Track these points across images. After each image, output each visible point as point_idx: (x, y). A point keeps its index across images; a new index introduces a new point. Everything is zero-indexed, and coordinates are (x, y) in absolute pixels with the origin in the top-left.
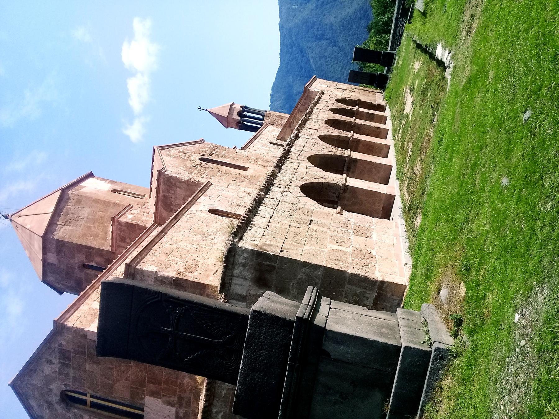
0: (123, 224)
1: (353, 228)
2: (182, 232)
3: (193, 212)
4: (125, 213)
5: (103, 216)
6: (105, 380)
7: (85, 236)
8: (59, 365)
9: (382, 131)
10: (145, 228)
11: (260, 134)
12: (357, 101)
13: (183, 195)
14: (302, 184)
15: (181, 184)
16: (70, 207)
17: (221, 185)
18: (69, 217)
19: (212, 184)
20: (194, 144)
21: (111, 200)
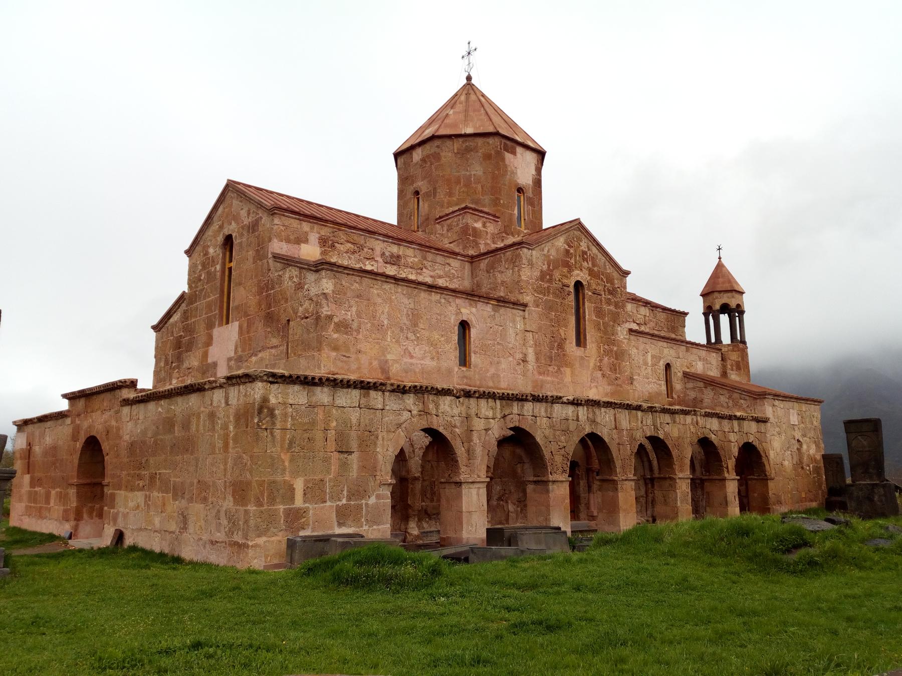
1: (352, 503)
2: (406, 301)
4: (483, 217)
5: (477, 192)
6: (244, 276)
8: (247, 223)
14: (441, 430)
19: (524, 311)
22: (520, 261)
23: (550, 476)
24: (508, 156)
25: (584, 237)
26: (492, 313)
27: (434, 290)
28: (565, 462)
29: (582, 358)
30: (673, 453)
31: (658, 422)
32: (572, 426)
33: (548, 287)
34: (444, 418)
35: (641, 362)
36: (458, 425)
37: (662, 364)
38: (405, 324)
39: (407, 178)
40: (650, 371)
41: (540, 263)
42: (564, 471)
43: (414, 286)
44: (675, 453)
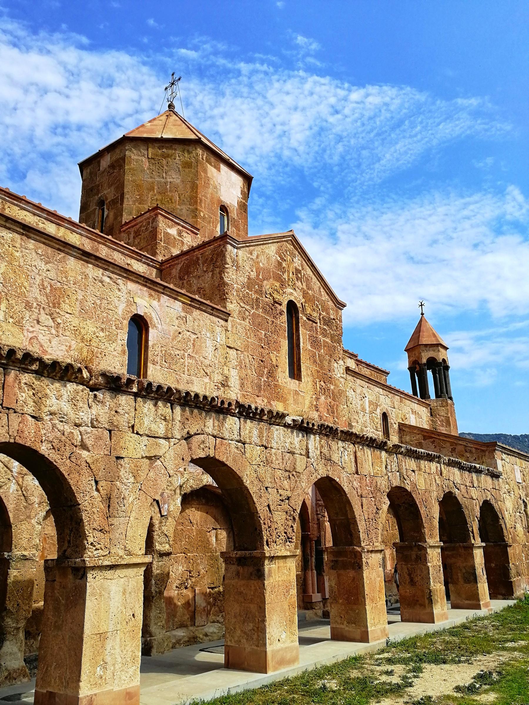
0: (154, 223)
2: (43, 266)
3: (122, 286)
4: (179, 224)
5: (173, 201)
7: (138, 187)
9: (428, 610)
10: (154, 254)
11: (401, 397)
12: (504, 541)
13: (203, 285)
14: (44, 449)
15: (218, 275)
16: (177, 158)
17: (230, 336)
18: (161, 161)
19: (226, 321)
20: (328, 294)
21: (203, 205)
22: (222, 260)
23: (266, 547)
24: (211, 170)
25: (297, 253)
26: (183, 314)
27: (93, 261)
28: (290, 523)
29: (296, 393)
30: (422, 512)
31: (404, 467)
32: (301, 463)
33: (257, 299)
34: (54, 426)
35: (359, 408)
36: (89, 443)
37: (379, 412)
38: (36, 298)
39: (92, 190)
40: (368, 418)
41: (247, 268)
42: (289, 539)
43: (57, 246)
44: (422, 510)
